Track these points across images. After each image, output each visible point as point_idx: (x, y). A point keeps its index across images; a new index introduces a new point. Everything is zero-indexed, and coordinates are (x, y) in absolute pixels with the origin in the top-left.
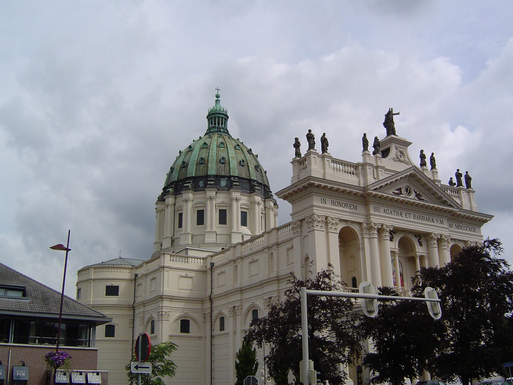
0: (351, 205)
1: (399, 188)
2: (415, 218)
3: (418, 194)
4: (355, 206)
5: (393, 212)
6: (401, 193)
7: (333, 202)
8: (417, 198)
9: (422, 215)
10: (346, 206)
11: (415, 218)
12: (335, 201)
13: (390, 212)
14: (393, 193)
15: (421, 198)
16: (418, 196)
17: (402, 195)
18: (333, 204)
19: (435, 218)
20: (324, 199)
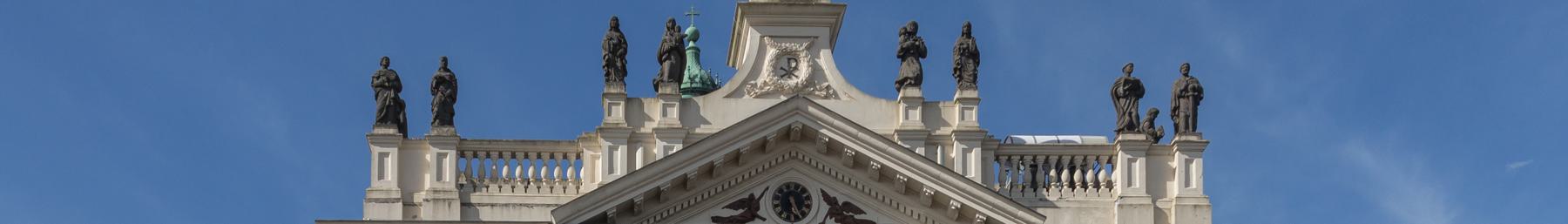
1: (746, 196)
3: (846, 204)
6: (754, 216)
15: (857, 217)
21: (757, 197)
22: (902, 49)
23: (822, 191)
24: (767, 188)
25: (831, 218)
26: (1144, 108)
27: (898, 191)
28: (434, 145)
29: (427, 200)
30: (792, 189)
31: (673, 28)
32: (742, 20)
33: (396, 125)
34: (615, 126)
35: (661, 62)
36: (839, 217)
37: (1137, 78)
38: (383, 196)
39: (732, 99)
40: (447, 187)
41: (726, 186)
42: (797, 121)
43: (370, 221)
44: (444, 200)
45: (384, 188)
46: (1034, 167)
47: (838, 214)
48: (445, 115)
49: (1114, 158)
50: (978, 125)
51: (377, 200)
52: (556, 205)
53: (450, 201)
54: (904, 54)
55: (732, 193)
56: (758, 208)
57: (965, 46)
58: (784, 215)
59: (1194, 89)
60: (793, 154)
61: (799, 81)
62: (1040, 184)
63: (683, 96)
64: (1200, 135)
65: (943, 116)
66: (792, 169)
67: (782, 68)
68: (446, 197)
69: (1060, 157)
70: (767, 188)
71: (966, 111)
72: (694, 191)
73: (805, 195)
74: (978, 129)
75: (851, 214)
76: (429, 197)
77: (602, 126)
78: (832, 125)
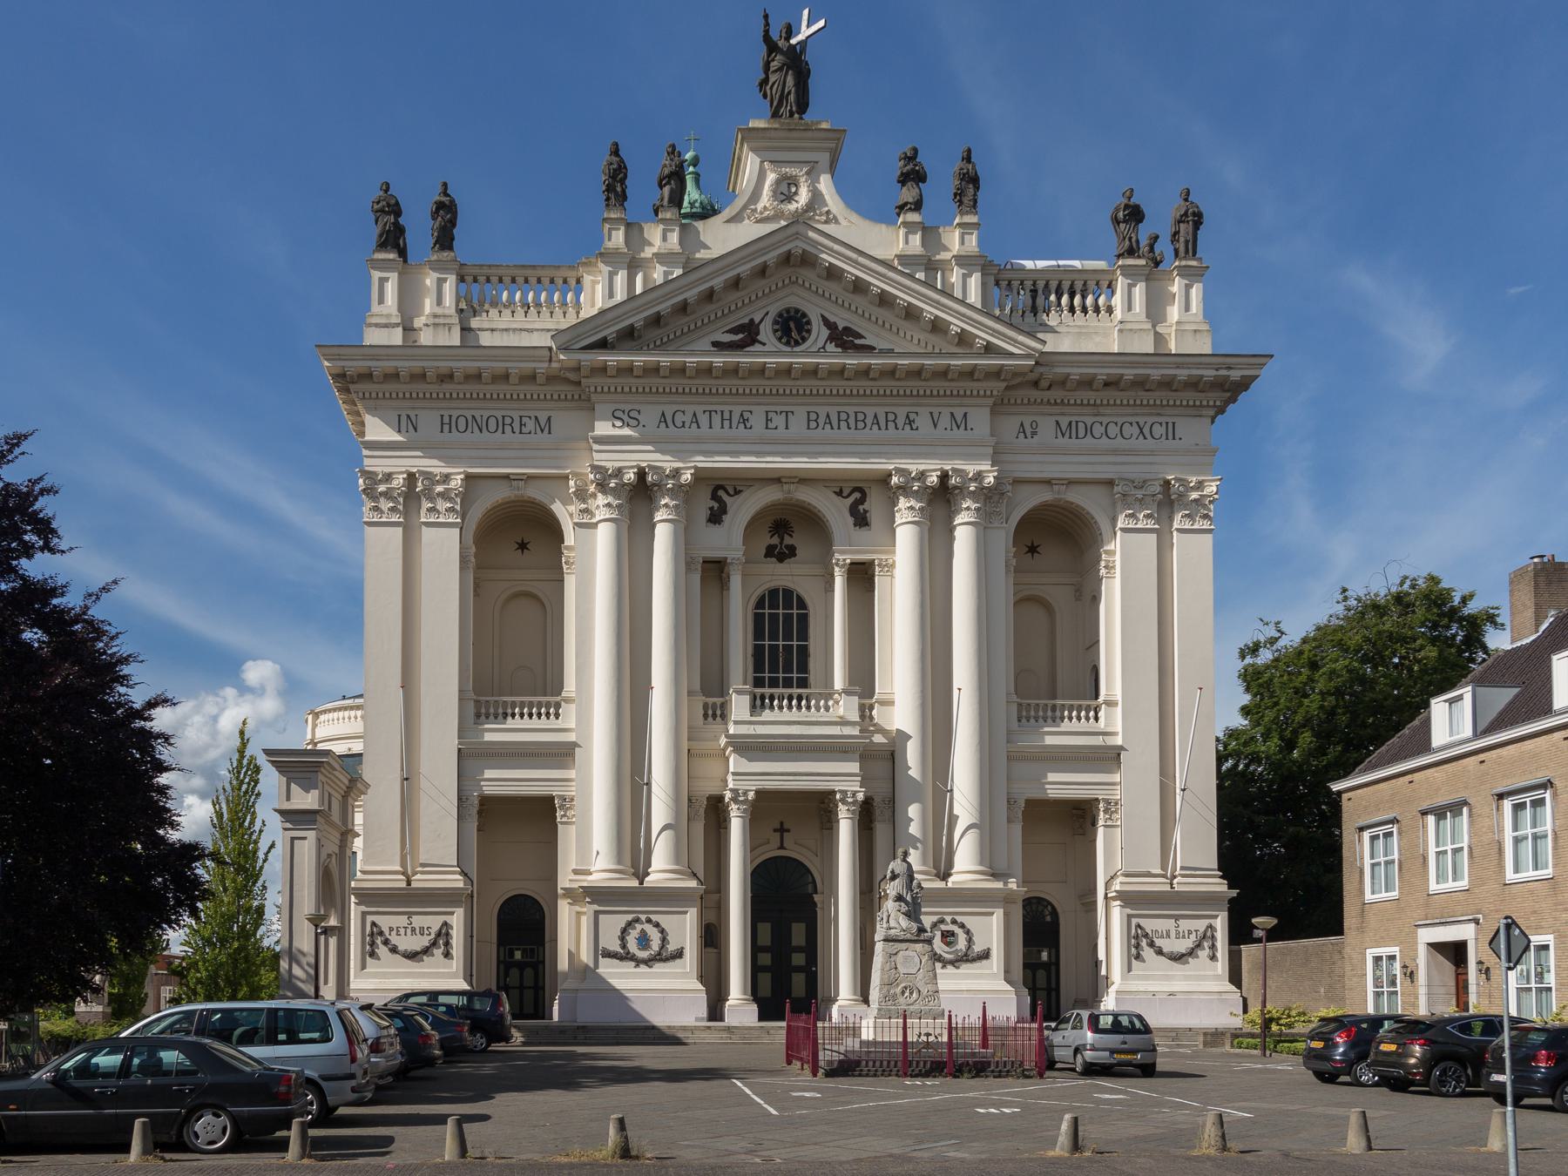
0: (524, 420)
1: (746, 320)
2: (813, 424)
3: (846, 329)
4: (543, 422)
5: (704, 419)
7: (446, 420)
8: (836, 346)
9: (851, 410)
10: (502, 425)
11: (813, 424)
12: (455, 414)
13: (688, 418)
14: (715, 344)
15: (857, 341)
16: (844, 338)
17: (757, 347)
18: (446, 428)
19: (924, 412)
20: (408, 416)
21: (757, 321)
22: (902, 174)
23: (822, 316)
24: (767, 313)
25: (831, 343)
26: (1144, 233)
27: (897, 316)
28: (434, 269)
29: (427, 325)
30: (792, 314)
31: (673, 153)
32: (742, 145)
33: (396, 250)
34: (614, 251)
35: (661, 187)
36: (839, 342)
37: (1137, 203)
38: (383, 321)
39: (732, 224)
40: (447, 312)
41: (726, 311)
42: (797, 246)
43: (370, 346)
44: (444, 324)
45: (384, 313)
46: (1034, 292)
47: (838, 339)
48: (445, 240)
49: (1114, 283)
50: (977, 249)
51: (377, 325)
52: (556, 330)
53: (450, 326)
54: (904, 179)
55: (733, 318)
56: (758, 334)
57: (965, 171)
58: (784, 340)
59: (1194, 214)
60: (794, 279)
61: (799, 205)
62: (1040, 308)
63: (683, 221)
64: (1200, 259)
65: (943, 241)
66: (792, 294)
67: (782, 193)
68: (446, 322)
69: (1073, 282)
70: (767, 313)
71: (966, 236)
72: (692, 317)
73: (804, 320)
74: (978, 254)
75: (851, 338)
76: (429, 322)
77: (603, 250)
78: (831, 250)
